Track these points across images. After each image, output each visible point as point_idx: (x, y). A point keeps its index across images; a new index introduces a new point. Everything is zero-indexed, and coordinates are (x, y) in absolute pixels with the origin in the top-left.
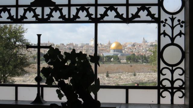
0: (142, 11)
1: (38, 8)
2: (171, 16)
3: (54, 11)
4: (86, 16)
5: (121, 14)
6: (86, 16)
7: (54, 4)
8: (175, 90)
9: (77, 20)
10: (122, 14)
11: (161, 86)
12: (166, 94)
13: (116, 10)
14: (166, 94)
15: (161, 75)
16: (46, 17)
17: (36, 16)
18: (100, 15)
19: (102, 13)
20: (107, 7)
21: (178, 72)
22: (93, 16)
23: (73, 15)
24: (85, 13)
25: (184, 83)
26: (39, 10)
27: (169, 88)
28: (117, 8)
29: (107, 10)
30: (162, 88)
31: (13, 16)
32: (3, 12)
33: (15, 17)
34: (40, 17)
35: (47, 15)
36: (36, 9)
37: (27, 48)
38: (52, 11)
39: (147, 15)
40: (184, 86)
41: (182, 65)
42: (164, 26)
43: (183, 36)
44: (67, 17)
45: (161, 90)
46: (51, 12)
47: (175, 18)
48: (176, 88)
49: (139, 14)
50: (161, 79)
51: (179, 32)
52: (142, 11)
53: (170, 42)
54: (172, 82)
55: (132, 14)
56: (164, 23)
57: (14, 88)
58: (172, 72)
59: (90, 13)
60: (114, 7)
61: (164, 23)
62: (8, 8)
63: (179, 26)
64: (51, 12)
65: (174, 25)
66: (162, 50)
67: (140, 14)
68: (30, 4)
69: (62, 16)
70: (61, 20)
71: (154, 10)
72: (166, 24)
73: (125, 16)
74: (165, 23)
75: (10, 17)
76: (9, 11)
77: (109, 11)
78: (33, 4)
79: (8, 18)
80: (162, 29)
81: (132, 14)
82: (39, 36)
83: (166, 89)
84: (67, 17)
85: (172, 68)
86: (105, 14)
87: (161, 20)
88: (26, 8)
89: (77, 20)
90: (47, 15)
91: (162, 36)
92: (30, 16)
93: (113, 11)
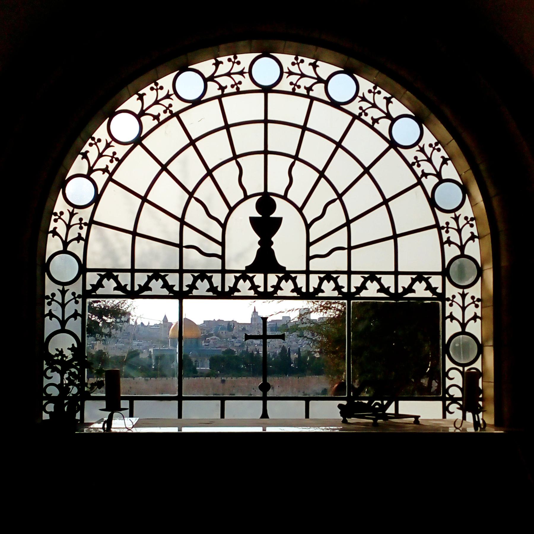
0: (418, 283)
2: (461, 291)
3: (284, 281)
4: (334, 290)
5: (386, 287)
6: (334, 290)
7: (282, 269)
9: (320, 295)
10: (389, 287)
11: (447, 396)
13: (379, 281)
15: (447, 379)
16: (270, 289)
17: (254, 287)
18: (356, 287)
19: (359, 285)
20: (366, 276)
22: (345, 290)
24: (332, 284)
26: (259, 279)
27: (459, 399)
28: (380, 278)
32: (199, 280)
33: (219, 289)
34: (261, 289)
35: (272, 287)
36: (254, 276)
37: (246, 339)
38: (280, 280)
39: (426, 289)
42: (451, 305)
43: (478, 320)
44: (304, 290)
45: (448, 402)
47: (467, 293)
49: (414, 287)
50: (447, 386)
51: (472, 315)
52: (418, 283)
53: (459, 329)
55: (403, 288)
56: (450, 302)
57: (219, 402)
59: (340, 284)
60: (376, 277)
61: (450, 302)
62: (209, 275)
65: (466, 305)
67: (414, 287)
68: (244, 269)
70: (295, 294)
71: (436, 281)
72: (454, 303)
74: (453, 301)
75: (212, 289)
76: (210, 279)
77: (369, 281)
78: (250, 269)
79: (208, 291)
80: (448, 310)
81: (403, 288)
83: (454, 400)
84: (304, 290)
85: (464, 369)
88: (238, 275)
90: (272, 287)
91: (448, 321)
92: (244, 287)
93: (375, 282)
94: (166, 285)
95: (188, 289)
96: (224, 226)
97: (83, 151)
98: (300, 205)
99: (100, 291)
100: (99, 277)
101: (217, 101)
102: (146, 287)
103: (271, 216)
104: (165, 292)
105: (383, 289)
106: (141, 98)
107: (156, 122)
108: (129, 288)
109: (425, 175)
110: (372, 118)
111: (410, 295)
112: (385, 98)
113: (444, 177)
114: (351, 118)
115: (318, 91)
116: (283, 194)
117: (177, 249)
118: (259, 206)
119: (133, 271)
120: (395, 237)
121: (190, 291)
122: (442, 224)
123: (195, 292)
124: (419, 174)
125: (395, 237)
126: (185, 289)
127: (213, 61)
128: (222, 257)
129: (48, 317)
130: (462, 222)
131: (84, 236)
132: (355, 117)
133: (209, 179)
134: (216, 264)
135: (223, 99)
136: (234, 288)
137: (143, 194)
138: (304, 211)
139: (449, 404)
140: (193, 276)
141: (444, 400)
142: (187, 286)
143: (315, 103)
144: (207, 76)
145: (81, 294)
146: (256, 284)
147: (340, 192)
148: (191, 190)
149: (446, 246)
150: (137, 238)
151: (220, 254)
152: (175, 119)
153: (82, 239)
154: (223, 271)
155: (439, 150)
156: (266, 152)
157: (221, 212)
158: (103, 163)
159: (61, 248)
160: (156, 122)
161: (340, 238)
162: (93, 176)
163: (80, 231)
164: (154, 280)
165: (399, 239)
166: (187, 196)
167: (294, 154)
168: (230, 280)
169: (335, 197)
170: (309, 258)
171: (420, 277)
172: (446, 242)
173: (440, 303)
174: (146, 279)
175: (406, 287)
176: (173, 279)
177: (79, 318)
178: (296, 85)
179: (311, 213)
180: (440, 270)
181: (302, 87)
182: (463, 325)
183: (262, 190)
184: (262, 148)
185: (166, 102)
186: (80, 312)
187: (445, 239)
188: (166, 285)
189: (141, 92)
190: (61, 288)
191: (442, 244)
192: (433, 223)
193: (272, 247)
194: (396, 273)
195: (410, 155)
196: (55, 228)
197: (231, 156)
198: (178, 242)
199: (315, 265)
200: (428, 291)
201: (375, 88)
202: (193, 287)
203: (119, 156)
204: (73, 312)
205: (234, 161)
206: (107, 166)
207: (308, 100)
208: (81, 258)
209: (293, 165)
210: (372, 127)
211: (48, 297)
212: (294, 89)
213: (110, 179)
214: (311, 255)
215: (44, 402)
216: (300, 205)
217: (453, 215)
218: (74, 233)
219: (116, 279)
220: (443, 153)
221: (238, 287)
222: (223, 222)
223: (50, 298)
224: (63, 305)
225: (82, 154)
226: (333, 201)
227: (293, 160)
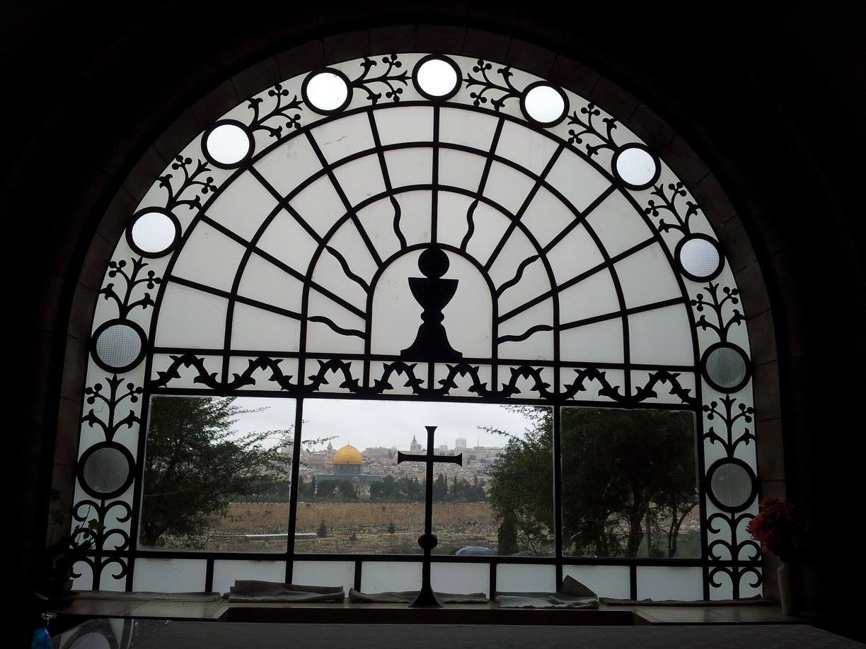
2: (724, 396)
4: (534, 389)
6: (534, 389)
8: (740, 569)
9: (513, 396)
10: (617, 388)
11: (710, 559)
12: (722, 577)
13: (602, 378)
14: (722, 577)
16: (438, 386)
17: (413, 382)
18: (566, 386)
20: (583, 369)
22: (551, 390)
23: (503, 384)
24: (531, 381)
26: (421, 370)
27: (727, 563)
30: (711, 564)
31: (358, 379)
33: (360, 384)
34: (424, 386)
36: (414, 366)
37: (399, 461)
38: (453, 373)
39: (672, 392)
42: (711, 417)
43: (752, 441)
44: (489, 388)
45: (711, 569)
48: (743, 563)
49: (655, 389)
50: (709, 543)
53: (724, 454)
54: (734, 549)
55: (638, 388)
56: (710, 412)
57: (351, 565)
58: (733, 524)
61: (710, 412)
62: (345, 362)
64: (451, 376)
66: (708, 471)
67: (655, 389)
69: (477, 386)
71: (686, 380)
72: (714, 414)
74: (713, 411)
75: (349, 383)
78: (407, 354)
79: (343, 386)
81: (638, 388)
82: (431, 430)
83: (720, 565)
84: (489, 388)
85: (733, 516)
88: (389, 363)
89: (513, 396)
91: (707, 441)
92: (398, 381)
93: (595, 379)
94: (278, 376)
95: (312, 382)
96: (370, 290)
97: (164, 174)
98: (483, 263)
100: (172, 361)
102: (246, 378)
104: (276, 386)
105: (607, 391)
106: (255, 105)
107: (275, 139)
108: (219, 379)
109: (665, 226)
111: (648, 400)
112: (605, 120)
113: (692, 231)
114: (556, 145)
115: (511, 107)
118: (423, 264)
119: (227, 353)
121: (315, 386)
122: (693, 297)
123: (323, 388)
124: (657, 225)
125: (624, 313)
126: (308, 382)
128: (366, 336)
131: (154, 297)
133: (349, 224)
134: (356, 345)
135: (376, 113)
138: (490, 273)
140: (321, 363)
142: (311, 378)
145: (142, 387)
146: (416, 378)
147: (543, 246)
148: (322, 235)
150: (238, 305)
152: (303, 137)
153: (151, 303)
154: (367, 357)
155: (683, 194)
156: (435, 187)
157: (366, 269)
158: (191, 193)
159: (117, 315)
160: (275, 139)
161: (543, 313)
162: (174, 211)
163: (149, 291)
165: (631, 318)
166: (315, 245)
167: (475, 190)
168: (377, 370)
170: (496, 341)
171: (663, 373)
173: (694, 413)
174: (247, 366)
176: (289, 368)
177: (136, 425)
178: (479, 98)
179: (500, 274)
180: (690, 362)
181: (489, 101)
182: (730, 448)
183: (429, 240)
184: (429, 181)
185: (292, 112)
186: (138, 414)
187: (697, 319)
188: (278, 376)
189: (255, 97)
191: (693, 326)
193: (442, 323)
194: (627, 367)
195: (643, 199)
197: (384, 190)
198: (298, 310)
202: (320, 379)
203: (217, 183)
205: (388, 199)
206: (198, 198)
207: (496, 120)
208: (147, 332)
210: (587, 158)
213: (201, 217)
214: (499, 336)
216: (483, 263)
218: (139, 292)
223: (94, 393)
224: (112, 404)
225: (161, 179)
227: (472, 200)
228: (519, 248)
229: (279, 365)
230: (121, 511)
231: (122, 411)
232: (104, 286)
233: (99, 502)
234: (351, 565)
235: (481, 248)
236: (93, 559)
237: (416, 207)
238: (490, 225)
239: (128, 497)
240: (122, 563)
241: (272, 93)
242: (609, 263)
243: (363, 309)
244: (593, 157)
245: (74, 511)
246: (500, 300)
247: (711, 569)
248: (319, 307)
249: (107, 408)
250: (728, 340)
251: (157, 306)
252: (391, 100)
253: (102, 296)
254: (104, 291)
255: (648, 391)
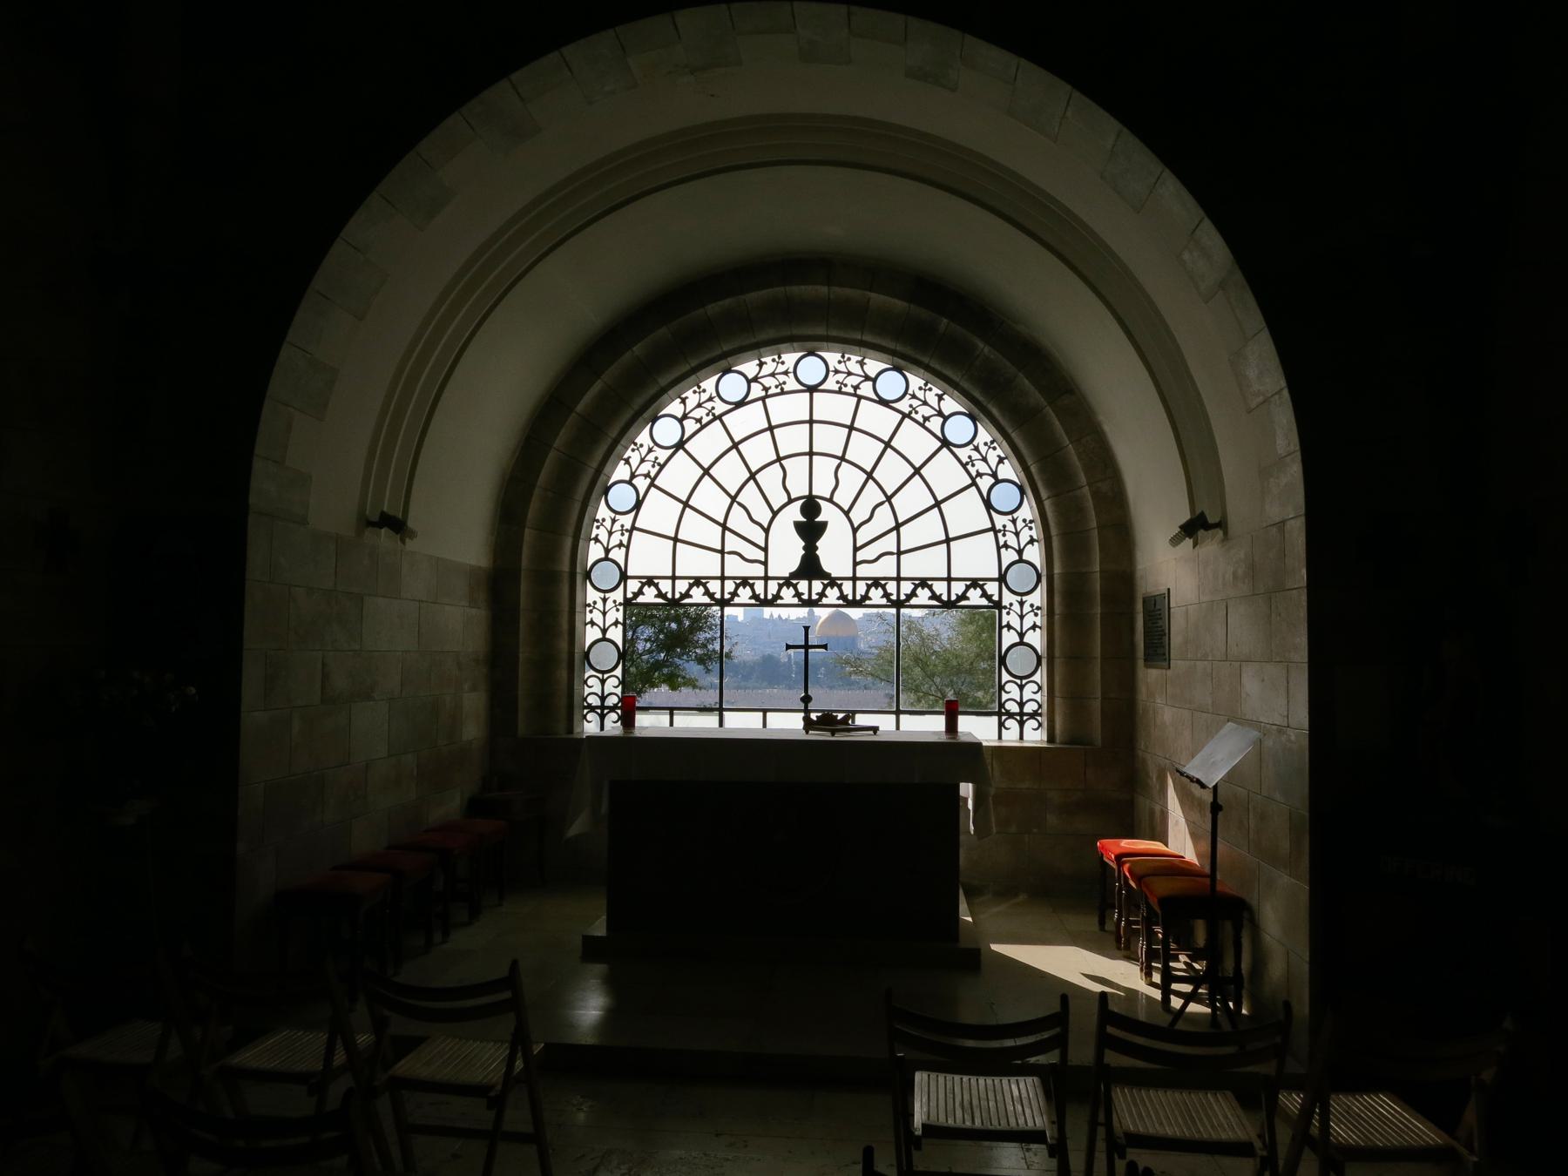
1: (802, 582)
2: (1019, 598)
4: (882, 597)
6: (882, 597)
8: (1025, 718)
9: (868, 602)
10: (941, 595)
11: (1003, 711)
14: (1012, 724)
15: (1003, 693)
16: (814, 597)
17: (798, 595)
18: (906, 595)
19: (909, 592)
20: (917, 582)
21: (1030, 689)
24: (880, 592)
25: (1040, 706)
26: (803, 586)
29: (916, 587)
30: (1004, 714)
33: (762, 597)
34: (805, 597)
35: (817, 594)
37: (787, 649)
38: (825, 587)
39: (981, 597)
40: (1040, 711)
41: (1037, 677)
42: (1008, 613)
44: (850, 597)
45: (1004, 718)
46: (824, 590)
48: (1027, 714)
49: (968, 595)
50: (1003, 700)
52: (972, 589)
53: (1017, 640)
54: (1021, 704)
55: (957, 595)
58: (1021, 687)
63: (1032, 613)
64: (824, 590)
67: (968, 595)
68: (788, 575)
69: (843, 597)
71: (992, 588)
73: (945, 598)
74: (1010, 609)
79: (750, 598)
81: (957, 595)
82: (807, 629)
83: (1011, 715)
84: (850, 597)
86: (913, 594)
87: (1004, 604)
88: (781, 582)
89: (868, 602)
90: (817, 594)
91: (1005, 630)
92: (788, 595)
93: (926, 589)
95: (730, 596)
96: (767, 531)
97: (626, 456)
98: (846, 508)
99: (640, 599)
101: (761, 402)
103: (817, 520)
106: (683, 401)
107: (698, 425)
108: (669, 596)
109: (979, 475)
110: (923, 416)
111: (963, 603)
115: (866, 389)
116: (828, 497)
117: (719, 555)
120: (948, 541)
121: (732, 599)
122: (999, 526)
124: (974, 474)
125: (948, 541)
126: (727, 596)
127: (757, 362)
128: (765, 563)
129: (589, 626)
130: (1020, 524)
131: (625, 543)
132: (905, 416)
133: (752, 481)
134: (758, 570)
136: (777, 596)
137: (684, 500)
138: (850, 515)
139: (1005, 720)
140: (735, 583)
141: (999, 714)
142: (729, 593)
143: (863, 401)
144: (750, 377)
145: (622, 602)
146: (800, 591)
147: (889, 494)
148: (733, 494)
149: (1003, 550)
150: (678, 544)
151: (763, 560)
153: (623, 545)
154: (766, 578)
155: (994, 449)
156: (811, 454)
157: (763, 516)
160: (698, 425)
161: (889, 543)
162: (634, 482)
164: (695, 587)
166: (729, 500)
167: (840, 455)
169: (885, 499)
170: (855, 564)
171: (975, 583)
172: (1003, 546)
173: (997, 611)
174: (687, 587)
175: (960, 594)
176: (714, 586)
179: (858, 516)
180: (996, 576)
183: (807, 493)
186: (621, 620)
187: (1001, 543)
188: (707, 593)
190: (602, 595)
191: (999, 548)
192: (990, 526)
193: (817, 552)
194: (949, 579)
195: (964, 454)
196: (597, 535)
198: (719, 548)
199: (862, 571)
200: (984, 599)
201: (926, 385)
202: (734, 594)
203: (661, 461)
204: (614, 620)
205: (778, 463)
207: (856, 399)
209: (838, 466)
210: (923, 426)
211: (589, 605)
212: (840, 388)
214: (858, 560)
215: (585, 711)
216: (846, 508)
217: (1010, 517)
219: (656, 586)
220: (999, 452)
221: (781, 594)
222: (766, 527)
224: (604, 613)
225: (625, 460)
226: (881, 504)
228: (872, 495)
229: (708, 585)
230: (616, 682)
231: (610, 619)
232: (593, 536)
233: (600, 676)
234: (761, 714)
235: (843, 498)
236: (599, 711)
237: (798, 468)
238: (851, 479)
239: (618, 672)
240: (617, 713)
241: (695, 392)
242: (938, 504)
243: (763, 545)
244: (927, 424)
245: (585, 682)
246: (858, 534)
247: (1004, 718)
248: (732, 543)
249: (601, 616)
250: (1024, 558)
251: (628, 548)
252: (778, 390)
253: (592, 542)
254: (594, 539)
255: (964, 597)
